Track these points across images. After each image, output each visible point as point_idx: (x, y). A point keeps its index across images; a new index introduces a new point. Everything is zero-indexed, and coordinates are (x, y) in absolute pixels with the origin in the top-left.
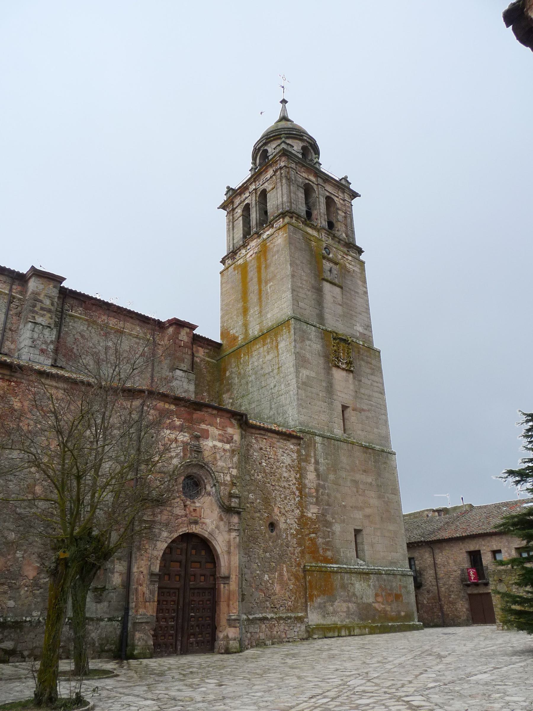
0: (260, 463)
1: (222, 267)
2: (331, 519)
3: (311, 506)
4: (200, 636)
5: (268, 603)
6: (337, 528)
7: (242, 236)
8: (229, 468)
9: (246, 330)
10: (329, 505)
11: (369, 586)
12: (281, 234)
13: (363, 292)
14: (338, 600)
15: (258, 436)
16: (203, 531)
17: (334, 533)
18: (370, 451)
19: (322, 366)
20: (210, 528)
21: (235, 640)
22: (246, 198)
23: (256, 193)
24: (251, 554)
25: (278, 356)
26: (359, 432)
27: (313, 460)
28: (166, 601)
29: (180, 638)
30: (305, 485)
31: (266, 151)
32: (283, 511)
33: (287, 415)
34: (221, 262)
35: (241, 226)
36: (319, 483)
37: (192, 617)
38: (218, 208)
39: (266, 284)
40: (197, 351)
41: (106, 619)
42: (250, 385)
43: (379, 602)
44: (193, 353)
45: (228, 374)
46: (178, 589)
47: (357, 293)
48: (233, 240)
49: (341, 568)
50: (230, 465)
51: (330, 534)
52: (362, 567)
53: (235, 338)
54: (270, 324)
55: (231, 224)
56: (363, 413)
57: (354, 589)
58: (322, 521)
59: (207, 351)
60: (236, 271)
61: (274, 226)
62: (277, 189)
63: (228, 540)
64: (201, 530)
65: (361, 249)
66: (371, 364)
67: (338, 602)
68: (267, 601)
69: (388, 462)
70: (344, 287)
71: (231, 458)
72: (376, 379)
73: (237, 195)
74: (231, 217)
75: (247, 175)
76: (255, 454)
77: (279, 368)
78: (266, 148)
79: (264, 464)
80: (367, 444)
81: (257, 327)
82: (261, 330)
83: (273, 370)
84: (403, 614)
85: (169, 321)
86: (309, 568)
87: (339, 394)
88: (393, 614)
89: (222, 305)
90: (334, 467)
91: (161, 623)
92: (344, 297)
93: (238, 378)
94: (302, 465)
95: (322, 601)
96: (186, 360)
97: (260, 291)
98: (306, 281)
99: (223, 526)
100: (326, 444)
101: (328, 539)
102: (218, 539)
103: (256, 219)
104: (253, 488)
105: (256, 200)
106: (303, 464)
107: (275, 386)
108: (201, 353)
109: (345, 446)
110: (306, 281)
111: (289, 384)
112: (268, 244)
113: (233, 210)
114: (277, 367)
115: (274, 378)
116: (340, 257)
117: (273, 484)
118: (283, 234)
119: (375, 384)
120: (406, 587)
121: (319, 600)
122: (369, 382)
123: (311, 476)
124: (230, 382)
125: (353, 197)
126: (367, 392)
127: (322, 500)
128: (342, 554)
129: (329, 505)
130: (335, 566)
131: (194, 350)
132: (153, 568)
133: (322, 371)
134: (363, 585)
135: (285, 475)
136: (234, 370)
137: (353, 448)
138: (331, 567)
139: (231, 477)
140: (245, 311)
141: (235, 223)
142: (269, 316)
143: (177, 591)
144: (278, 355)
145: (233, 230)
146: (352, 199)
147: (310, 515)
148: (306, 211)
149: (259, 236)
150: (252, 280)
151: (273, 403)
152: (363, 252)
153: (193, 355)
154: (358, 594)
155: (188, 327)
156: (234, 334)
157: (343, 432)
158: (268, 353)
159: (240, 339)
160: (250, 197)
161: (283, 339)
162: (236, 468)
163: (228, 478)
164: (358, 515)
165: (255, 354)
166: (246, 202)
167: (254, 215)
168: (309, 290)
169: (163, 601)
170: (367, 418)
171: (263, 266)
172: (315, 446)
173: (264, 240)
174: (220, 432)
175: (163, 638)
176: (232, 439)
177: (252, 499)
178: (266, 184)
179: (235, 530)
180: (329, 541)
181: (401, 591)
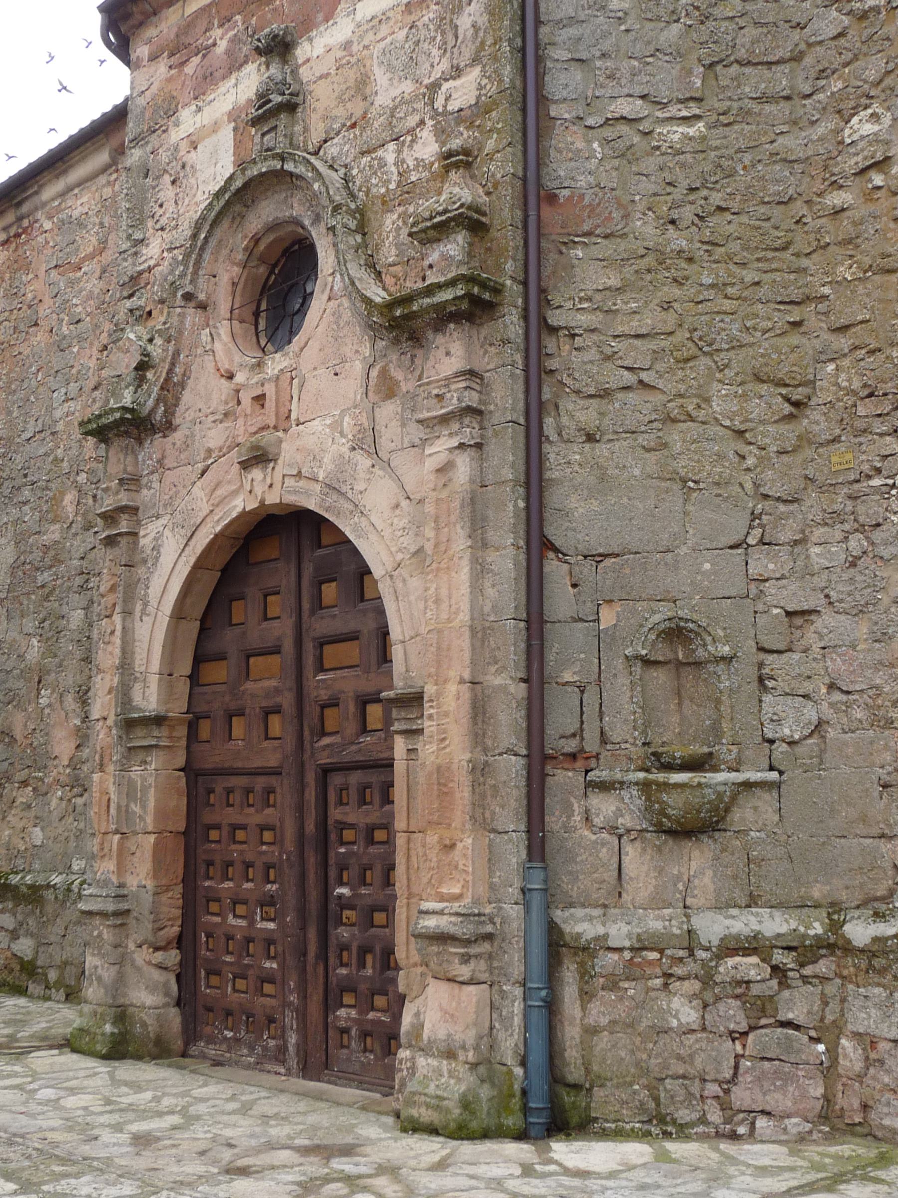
8: (434, 87)
16: (302, 483)
21: (450, 1054)
37: (344, 904)
50: (444, 65)
99: (395, 424)
102: (367, 501)
139: (441, 133)
162: (476, 60)
175: (241, 984)
179: (444, 420)
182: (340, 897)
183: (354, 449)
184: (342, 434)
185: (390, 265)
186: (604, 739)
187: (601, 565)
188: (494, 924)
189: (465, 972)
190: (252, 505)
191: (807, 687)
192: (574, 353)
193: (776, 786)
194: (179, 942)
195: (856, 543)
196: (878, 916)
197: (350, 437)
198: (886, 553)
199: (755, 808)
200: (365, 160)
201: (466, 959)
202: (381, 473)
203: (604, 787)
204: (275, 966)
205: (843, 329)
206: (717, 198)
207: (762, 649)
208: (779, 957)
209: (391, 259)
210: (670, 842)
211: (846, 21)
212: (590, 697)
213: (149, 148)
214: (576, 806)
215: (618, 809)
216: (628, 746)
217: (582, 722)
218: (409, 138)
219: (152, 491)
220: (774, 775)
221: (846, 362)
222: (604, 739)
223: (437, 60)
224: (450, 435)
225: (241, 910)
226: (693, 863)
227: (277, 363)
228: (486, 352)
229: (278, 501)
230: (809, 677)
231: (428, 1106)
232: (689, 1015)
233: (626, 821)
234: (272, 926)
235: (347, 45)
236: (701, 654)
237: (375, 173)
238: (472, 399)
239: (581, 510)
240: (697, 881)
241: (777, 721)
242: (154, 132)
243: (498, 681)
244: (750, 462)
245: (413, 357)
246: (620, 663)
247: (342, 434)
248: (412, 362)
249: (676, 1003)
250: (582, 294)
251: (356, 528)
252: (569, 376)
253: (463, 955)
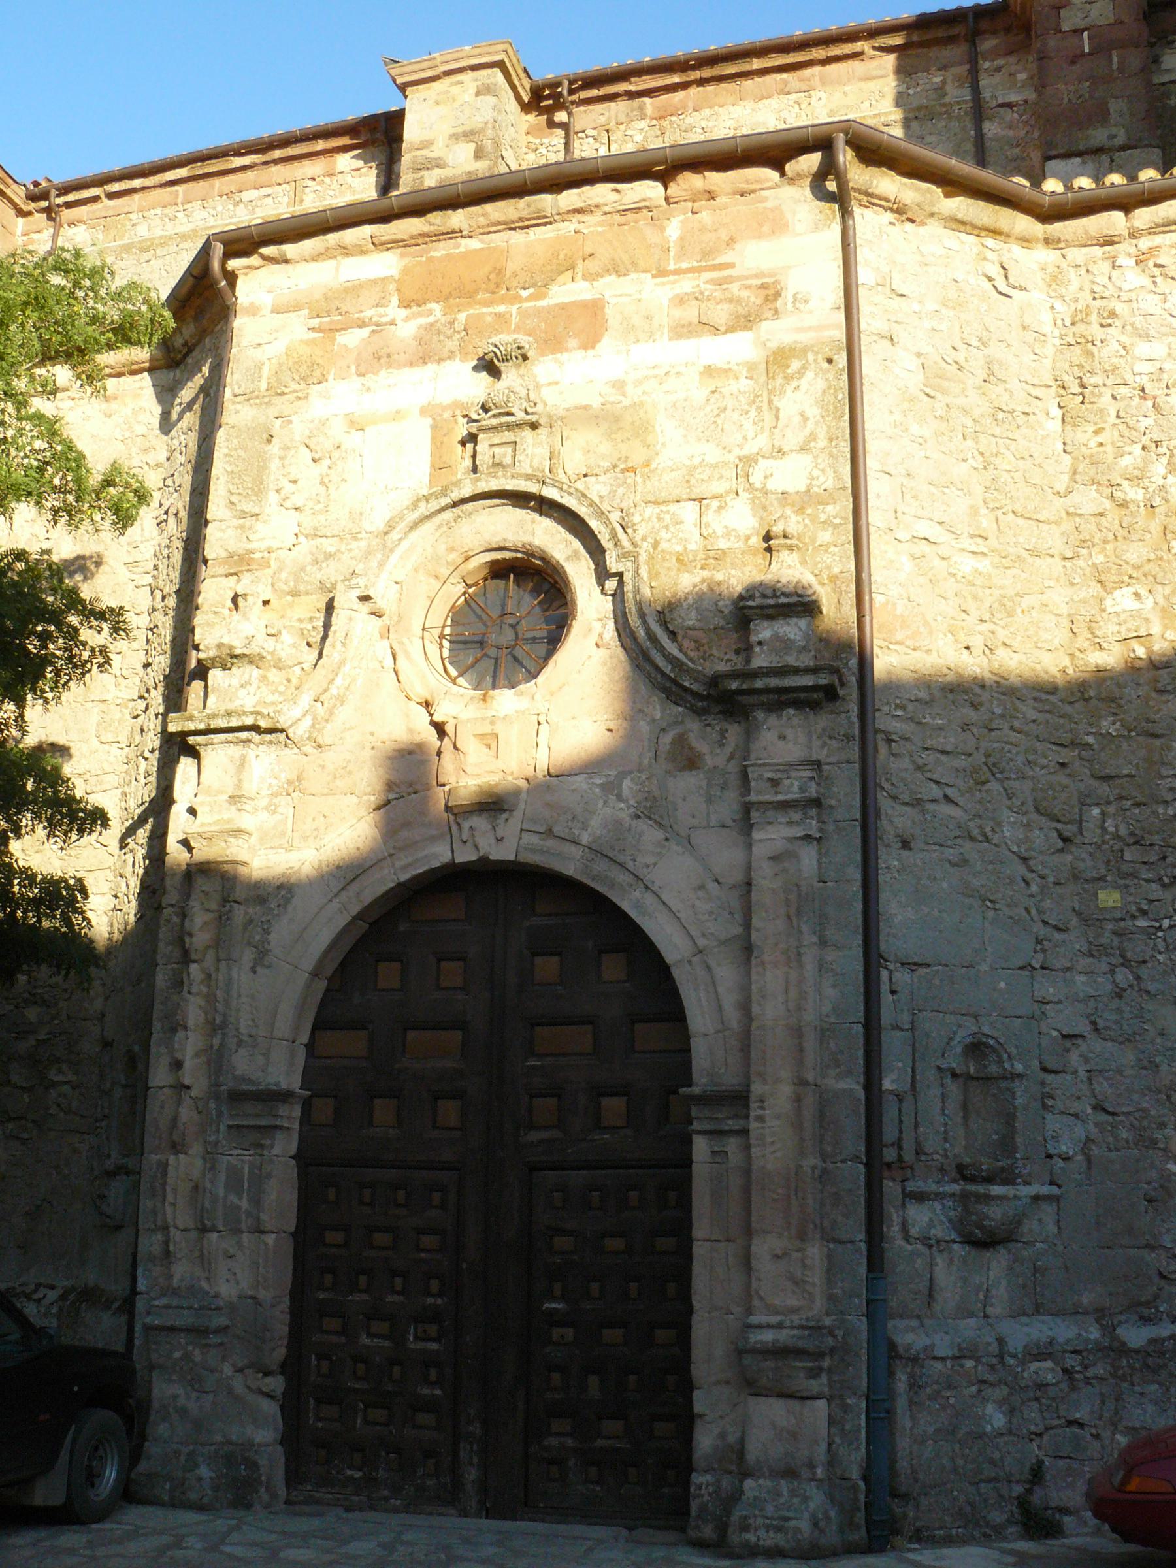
4: (612, 1426)
8: (748, 461)
15: (1158, 240)
16: (550, 843)
20: (595, 823)
21: (790, 1473)
24: (1137, 948)
29: (476, 1428)
50: (762, 442)
63: (738, 877)
64: (534, 840)
76: (1142, 349)
96: (1114, 106)
104: (1135, 553)
132: (243, 1064)
162: (804, 448)
174: (687, 285)
175: (379, 1414)
177: (1136, 615)
179: (785, 806)
182: (552, 1312)
183: (638, 817)
184: (619, 798)
185: (690, 629)
186: (919, 1151)
187: (917, 973)
188: (834, 1336)
189: (814, 1386)
190: (465, 856)
191: (1076, 1107)
192: (892, 759)
193: (1056, 1199)
194: (284, 1367)
196: (1145, 1320)
197: (632, 802)
198: (1152, 987)
199: (1040, 1220)
200: (650, 511)
201: (814, 1374)
202: (680, 849)
203: (921, 1197)
204: (438, 1392)
205: (1107, 778)
206: (1002, 635)
207: (1045, 1070)
208: (1071, 1361)
209: (691, 623)
210: (973, 1253)
211: (1108, 504)
212: (908, 1105)
213: (272, 411)
214: (895, 1217)
215: (931, 1220)
216: (938, 1157)
217: (901, 1132)
218: (715, 504)
219: (278, 817)
220: (1054, 1190)
221: (1111, 809)
222: (919, 1151)
223: (750, 435)
224: (790, 823)
225: (382, 1327)
226: (991, 1273)
227: (505, 700)
228: (825, 744)
229: (512, 858)
230: (1079, 1098)
231: (768, 1528)
232: (999, 1420)
233: (938, 1232)
234: (434, 1346)
236: (993, 1069)
237: (667, 527)
238: (813, 791)
239: (900, 917)
240: (994, 1292)
241: (1056, 1138)
242: (283, 394)
243: (843, 1085)
244: (1034, 888)
245: (723, 733)
246: (932, 1075)
247: (619, 798)
248: (723, 736)
249: (990, 1408)
250: (898, 701)
251: (638, 905)
252: (887, 780)
253: (811, 1369)
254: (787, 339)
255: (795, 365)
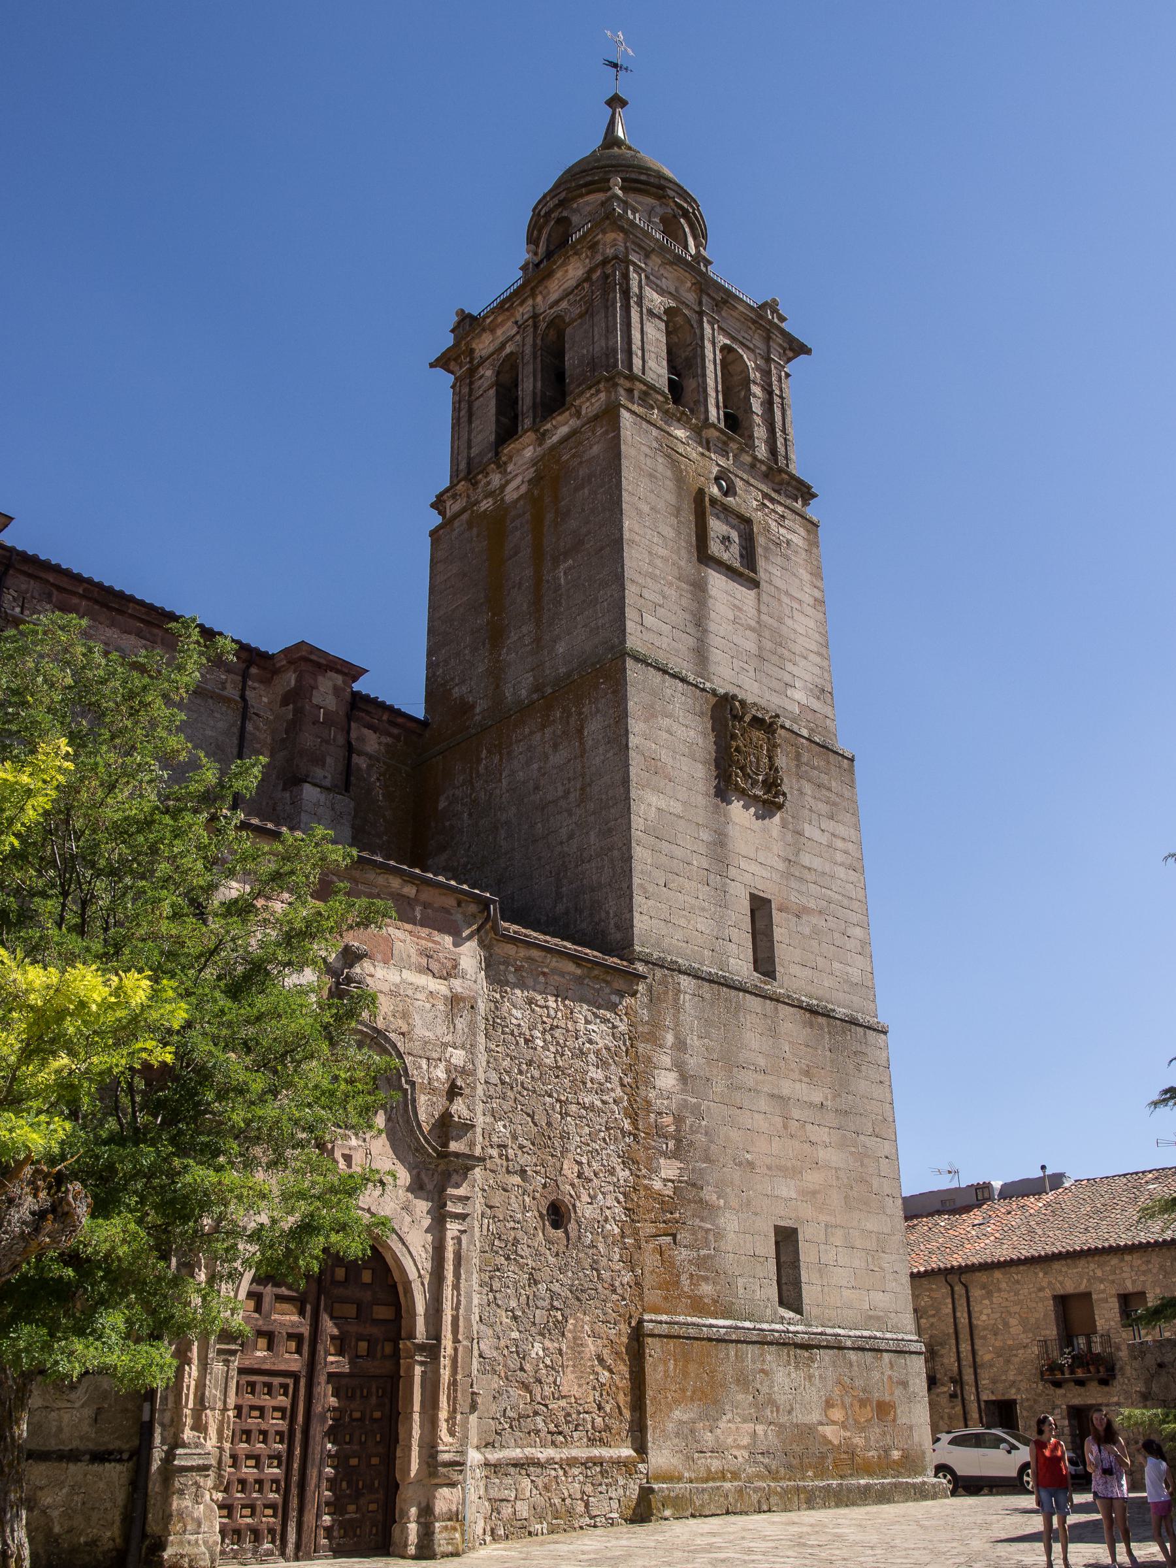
0: (527, 1041)
1: (437, 520)
2: (714, 1197)
3: (662, 1161)
4: (352, 1508)
5: (539, 1419)
6: (730, 1222)
7: (492, 438)
8: (445, 1045)
9: (498, 686)
10: (707, 1159)
11: (810, 1377)
12: (599, 432)
13: (812, 602)
14: (729, 1416)
17: (719, 1235)
18: (821, 1020)
19: (701, 786)
22: (511, 338)
23: (535, 327)
25: (582, 756)
26: (795, 970)
27: (670, 1038)
28: (261, 1409)
30: (648, 1103)
31: (564, 222)
32: (588, 1173)
33: (603, 915)
34: (433, 506)
35: (493, 410)
36: (685, 1100)
38: (432, 365)
39: (556, 562)
40: (361, 739)
41: (87, 1457)
42: (503, 833)
43: (834, 1423)
44: (349, 743)
45: (442, 804)
46: (295, 1376)
47: (800, 602)
48: (469, 447)
49: (737, 1328)
50: (448, 1038)
51: (711, 1237)
52: (792, 1328)
53: (465, 708)
54: (562, 670)
55: (464, 405)
56: (805, 917)
57: (771, 1387)
58: (689, 1201)
59: (389, 740)
60: (475, 531)
61: (583, 412)
62: (592, 316)
65: (809, 487)
66: (829, 789)
67: (729, 1421)
68: (536, 1413)
69: (868, 1050)
70: (763, 584)
71: (451, 1017)
72: (842, 830)
73: (484, 330)
74: (465, 390)
75: (512, 277)
77: (583, 789)
78: (565, 214)
79: (540, 1043)
80: (815, 1002)
81: (528, 679)
82: (537, 688)
83: (567, 793)
84: (896, 1454)
85: (286, 651)
86: (651, 1326)
87: (744, 864)
88: (871, 1454)
89: (431, 620)
90: (729, 1061)
91: (245, 1470)
92: (764, 608)
93: (470, 815)
94: (640, 1050)
95: (685, 1418)
96: (329, 760)
97: (538, 581)
98: (665, 559)
100: (707, 996)
101: (703, 1252)
103: (534, 394)
105: (534, 345)
106: (642, 1047)
107: (571, 836)
108: (372, 742)
109: (753, 1002)
110: (665, 559)
111: (610, 830)
112: (565, 458)
113: (472, 371)
114: (578, 786)
115: (570, 815)
116: (755, 503)
117: (563, 1098)
118: (606, 432)
119: (839, 844)
120: (904, 1384)
121: (677, 1414)
122: (824, 839)
123: (667, 1080)
124: (447, 824)
125: (791, 354)
126: (816, 863)
127: (691, 1144)
128: (741, 1291)
129: (707, 1159)
130: (721, 1322)
131: (353, 735)
133: (701, 800)
134: (793, 1375)
135: (594, 1076)
136: (458, 793)
137: (776, 1009)
138: (711, 1326)
139: (448, 1071)
140: (496, 635)
141: (477, 404)
142: (561, 650)
143: (290, 1381)
144: (583, 752)
145: (470, 422)
146: (789, 360)
147: (657, 1185)
148: (670, 380)
149: (542, 438)
150: (516, 554)
151: (565, 881)
152: (814, 496)
153: (350, 749)
154: (781, 1399)
155: (338, 671)
156: (462, 698)
157: (751, 966)
158: (555, 746)
159: (478, 710)
160: (518, 337)
161: (598, 711)
162: (463, 1047)
163: (440, 1073)
164: (786, 1189)
165: (518, 749)
166: (508, 350)
167: (529, 386)
168: (671, 584)
169: (252, 1408)
170: (816, 931)
171: (549, 517)
172: (676, 1000)
173: (553, 448)
176: (455, 967)
178: (564, 304)
180: (708, 1256)
181: (892, 1394)
195: (491, 1295)
235: (397, 986)
254: (460, 990)
255: (462, 1005)
